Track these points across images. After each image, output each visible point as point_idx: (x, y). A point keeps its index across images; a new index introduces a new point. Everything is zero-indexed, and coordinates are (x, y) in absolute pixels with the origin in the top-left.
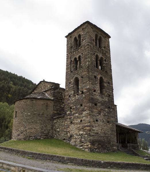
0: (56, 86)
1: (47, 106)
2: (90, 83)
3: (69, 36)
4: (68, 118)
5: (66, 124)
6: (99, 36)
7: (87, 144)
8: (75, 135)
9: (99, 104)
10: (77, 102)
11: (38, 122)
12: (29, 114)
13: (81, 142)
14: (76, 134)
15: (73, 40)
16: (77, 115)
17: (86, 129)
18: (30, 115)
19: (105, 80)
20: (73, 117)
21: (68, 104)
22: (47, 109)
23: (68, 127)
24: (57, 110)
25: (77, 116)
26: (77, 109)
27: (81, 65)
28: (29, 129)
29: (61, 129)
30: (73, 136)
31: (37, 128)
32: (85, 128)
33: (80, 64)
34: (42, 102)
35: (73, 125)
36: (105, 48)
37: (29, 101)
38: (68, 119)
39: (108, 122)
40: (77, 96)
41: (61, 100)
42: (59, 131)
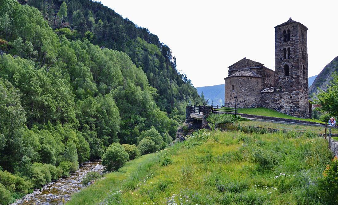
0: (260, 67)
1: (258, 82)
2: (299, 71)
3: (278, 28)
4: (278, 94)
5: (276, 98)
6: (302, 31)
7: (296, 113)
8: (284, 106)
9: (302, 86)
10: (286, 84)
11: (253, 95)
12: (247, 89)
13: (290, 111)
14: (286, 106)
15: (282, 32)
16: (287, 92)
17: (295, 103)
18: (247, 90)
19: (305, 66)
20: (283, 94)
21: (278, 83)
22: (258, 85)
23: (278, 101)
24: (263, 86)
25: (287, 94)
26: (286, 88)
27: (291, 55)
28: (247, 100)
29: (270, 101)
30: (283, 107)
31: (252, 99)
32: (294, 103)
33: (289, 54)
34: (254, 80)
35: (282, 99)
36: (305, 40)
37: (246, 78)
38: (278, 94)
39: (306, 98)
40: (287, 79)
41: (265, 77)
42: (267, 103)
